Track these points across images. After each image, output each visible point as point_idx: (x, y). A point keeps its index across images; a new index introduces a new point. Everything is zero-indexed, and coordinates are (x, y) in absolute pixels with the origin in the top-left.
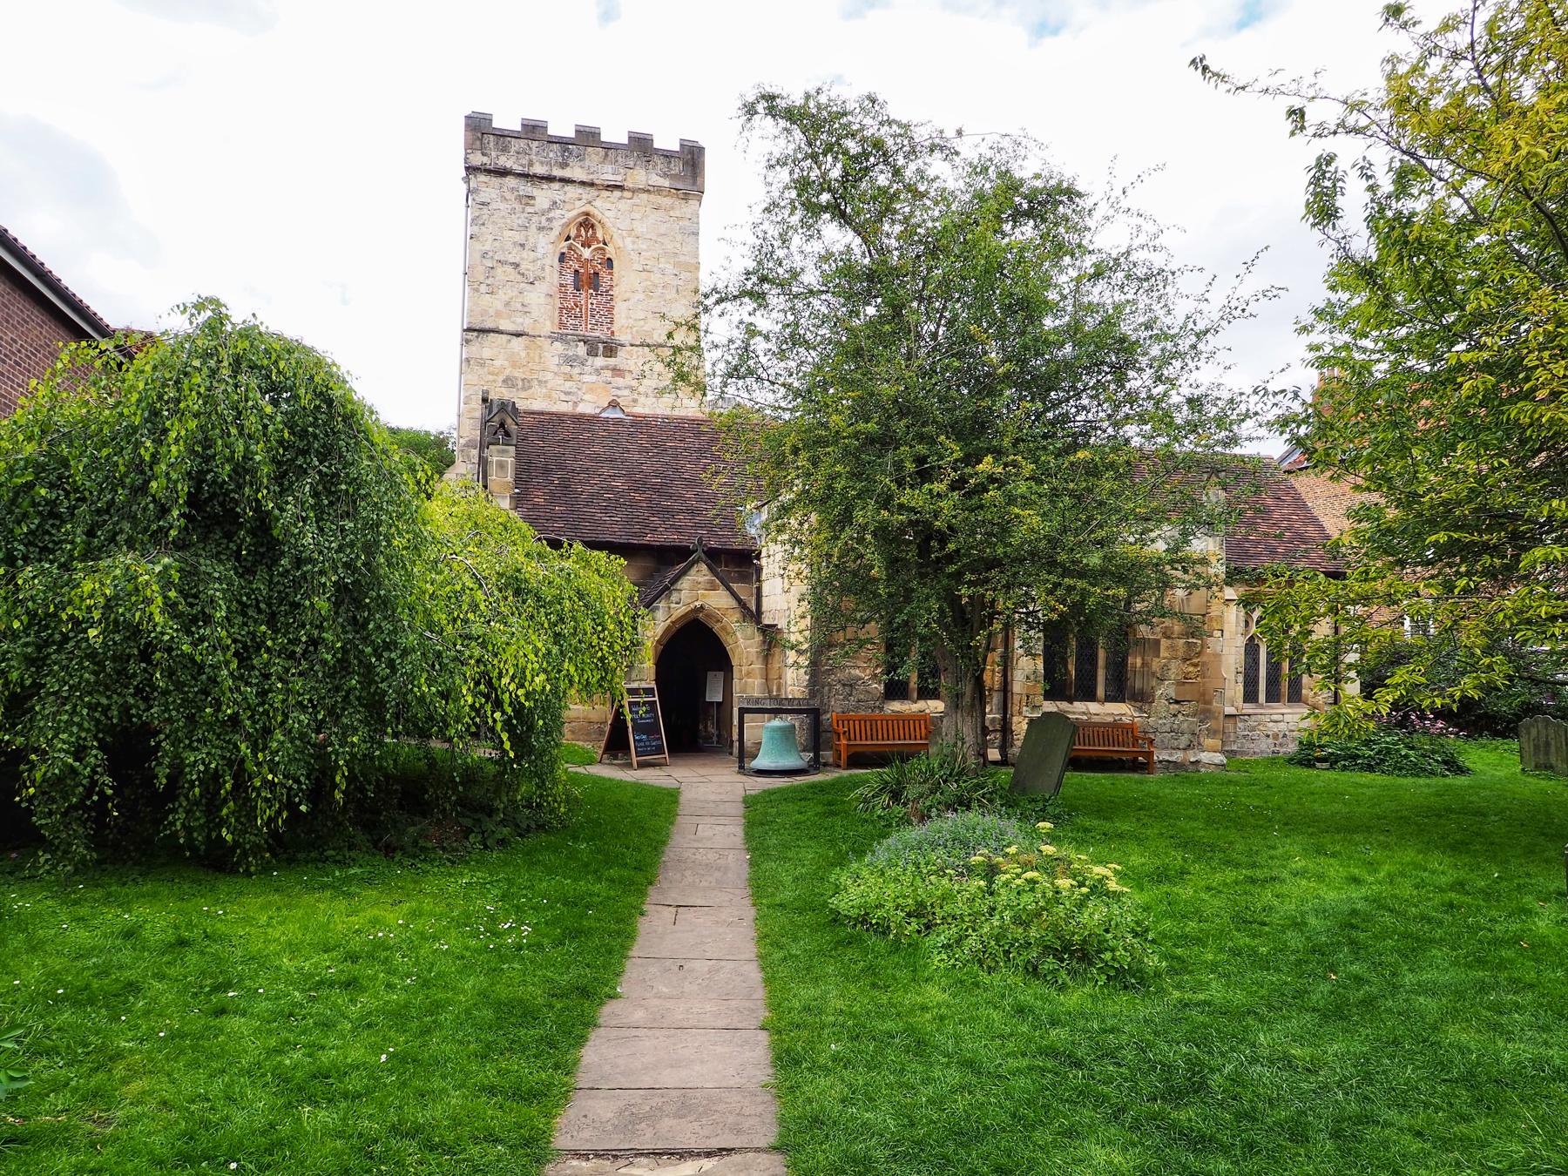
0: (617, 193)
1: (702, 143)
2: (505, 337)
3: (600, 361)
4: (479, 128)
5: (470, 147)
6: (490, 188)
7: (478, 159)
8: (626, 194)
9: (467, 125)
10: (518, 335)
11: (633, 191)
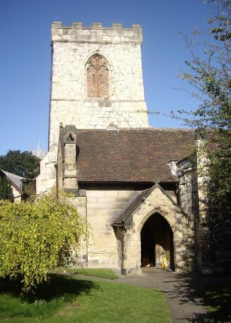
0: (109, 45)
2: (66, 102)
3: (105, 109)
8: (113, 45)
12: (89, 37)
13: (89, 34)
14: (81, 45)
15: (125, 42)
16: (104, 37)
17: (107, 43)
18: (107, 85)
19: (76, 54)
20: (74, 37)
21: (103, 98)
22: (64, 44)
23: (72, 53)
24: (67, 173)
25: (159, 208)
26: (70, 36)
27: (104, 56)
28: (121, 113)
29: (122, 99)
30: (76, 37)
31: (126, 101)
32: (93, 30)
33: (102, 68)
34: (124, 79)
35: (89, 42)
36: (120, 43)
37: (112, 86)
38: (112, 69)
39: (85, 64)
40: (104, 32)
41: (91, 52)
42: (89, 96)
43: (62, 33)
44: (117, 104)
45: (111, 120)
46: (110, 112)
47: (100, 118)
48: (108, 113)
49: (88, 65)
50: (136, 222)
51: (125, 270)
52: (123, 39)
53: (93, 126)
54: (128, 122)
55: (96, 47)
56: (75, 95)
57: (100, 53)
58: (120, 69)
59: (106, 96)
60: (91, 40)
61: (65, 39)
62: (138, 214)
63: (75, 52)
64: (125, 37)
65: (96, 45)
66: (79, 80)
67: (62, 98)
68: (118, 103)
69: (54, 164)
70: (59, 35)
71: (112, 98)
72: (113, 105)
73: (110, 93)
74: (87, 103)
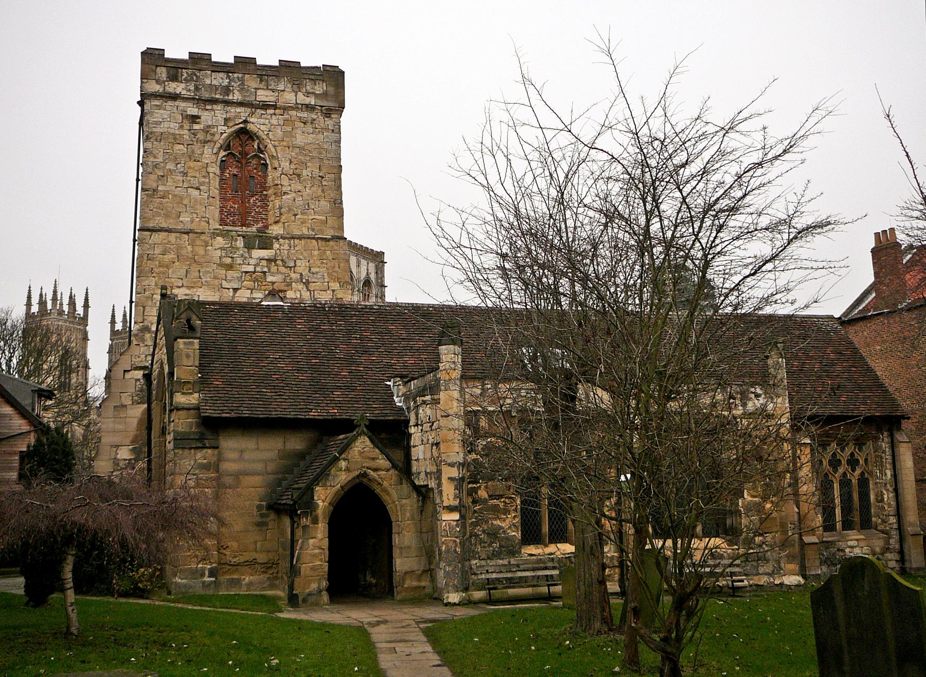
3: (258, 253)
4: (152, 59)
5: (144, 77)
7: (154, 87)
8: (277, 111)
10: (187, 233)
11: (285, 109)
12: (227, 90)
14: (208, 107)
15: (307, 106)
16: (259, 92)
17: (265, 106)
18: (265, 199)
19: (196, 127)
20: (192, 88)
21: (254, 229)
22: (170, 103)
23: (187, 126)
26: (183, 85)
27: (260, 133)
28: (292, 264)
29: (297, 232)
30: (197, 88)
31: (304, 238)
32: (236, 75)
33: (254, 162)
34: (300, 187)
35: (228, 103)
36: (297, 107)
40: (261, 81)
42: (223, 222)
43: (164, 76)
45: (270, 278)
46: (269, 260)
48: (264, 263)
50: (320, 503)
52: (302, 98)
53: (231, 293)
54: (307, 284)
55: (243, 112)
56: (192, 221)
57: (250, 127)
58: (293, 166)
59: (260, 225)
60: (230, 97)
61: (171, 90)
62: (324, 485)
64: (308, 94)
66: (202, 188)
67: (164, 225)
68: (287, 241)
69: (142, 372)
70: (158, 82)
71: (276, 230)
72: (276, 246)
73: (271, 220)
74: (220, 239)
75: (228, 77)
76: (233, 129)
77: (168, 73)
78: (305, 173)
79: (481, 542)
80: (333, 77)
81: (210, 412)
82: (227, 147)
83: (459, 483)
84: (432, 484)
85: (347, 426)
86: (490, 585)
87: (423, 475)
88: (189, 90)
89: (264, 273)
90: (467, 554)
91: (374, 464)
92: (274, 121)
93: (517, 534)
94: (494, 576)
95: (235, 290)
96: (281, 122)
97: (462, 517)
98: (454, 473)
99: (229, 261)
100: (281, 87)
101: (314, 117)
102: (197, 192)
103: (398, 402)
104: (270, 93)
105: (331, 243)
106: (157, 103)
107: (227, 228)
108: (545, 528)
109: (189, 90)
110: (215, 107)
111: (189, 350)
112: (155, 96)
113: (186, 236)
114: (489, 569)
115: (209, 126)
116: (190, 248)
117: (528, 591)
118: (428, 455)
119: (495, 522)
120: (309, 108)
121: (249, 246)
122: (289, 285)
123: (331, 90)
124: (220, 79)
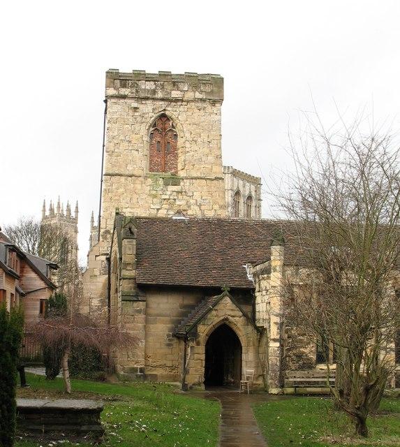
0: (179, 103)
1: (222, 76)
2: (123, 179)
3: (171, 188)
6: (117, 108)
7: (112, 92)
8: (184, 103)
9: (107, 76)
10: (131, 176)
11: (188, 102)
12: (154, 92)
13: (153, 87)
14: (143, 102)
15: (201, 99)
17: (176, 100)
18: (176, 156)
19: (137, 114)
20: (134, 91)
22: (122, 101)
23: (131, 113)
24: (126, 273)
25: (227, 319)
26: (129, 90)
27: (173, 116)
29: (195, 175)
30: (137, 91)
33: (170, 133)
36: (195, 100)
37: (181, 158)
38: (182, 134)
39: (147, 128)
40: (174, 85)
41: (156, 111)
42: (151, 170)
43: (119, 85)
44: (187, 182)
46: (178, 192)
47: (164, 199)
48: (175, 193)
49: (152, 129)
51: (187, 385)
52: (198, 95)
54: (200, 206)
57: (167, 113)
58: (192, 136)
59: (173, 171)
60: (156, 96)
61: (122, 93)
63: (135, 111)
64: (201, 92)
65: (163, 102)
68: (188, 181)
71: (182, 174)
72: (182, 184)
73: (180, 167)
75: (155, 84)
76: (158, 115)
77: (121, 83)
78: (199, 140)
79: (292, 360)
80: (217, 82)
81: (141, 281)
82: (155, 125)
83: (281, 325)
84: (266, 326)
85: (217, 291)
86: (296, 385)
87: (261, 321)
88: (132, 93)
89: (175, 199)
90: (284, 366)
91: (232, 313)
92: (182, 109)
93: (314, 357)
94: (298, 380)
95: (158, 210)
96: (186, 110)
97: (282, 346)
98: (277, 320)
99: (154, 192)
100: (186, 89)
101: (205, 106)
102: (136, 153)
103: (250, 277)
104: (179, 92)
105: (214, 182)
106: (113, 100)
107: (153, 173)
108: (331, 356)
109: (132, 93)
110: (147, 102)
111: (130, 247)
112: (112, 97)
113: (130, 178)
114: (295, 376)
115: (144, 114)
116: (132, 185)
117: (319, 390)
118: (265, 309)
119: (301, 349)
120: (202, 100)
121: (166, 184)
122: (189, 207)
123: (215, 89)
124: (150, 86)
